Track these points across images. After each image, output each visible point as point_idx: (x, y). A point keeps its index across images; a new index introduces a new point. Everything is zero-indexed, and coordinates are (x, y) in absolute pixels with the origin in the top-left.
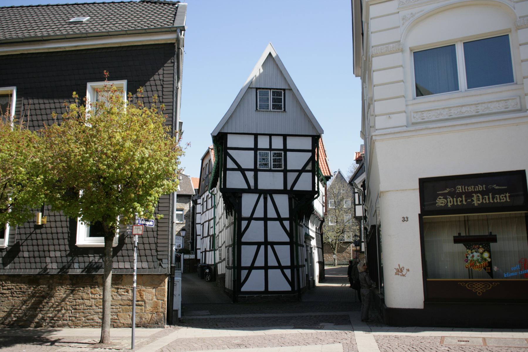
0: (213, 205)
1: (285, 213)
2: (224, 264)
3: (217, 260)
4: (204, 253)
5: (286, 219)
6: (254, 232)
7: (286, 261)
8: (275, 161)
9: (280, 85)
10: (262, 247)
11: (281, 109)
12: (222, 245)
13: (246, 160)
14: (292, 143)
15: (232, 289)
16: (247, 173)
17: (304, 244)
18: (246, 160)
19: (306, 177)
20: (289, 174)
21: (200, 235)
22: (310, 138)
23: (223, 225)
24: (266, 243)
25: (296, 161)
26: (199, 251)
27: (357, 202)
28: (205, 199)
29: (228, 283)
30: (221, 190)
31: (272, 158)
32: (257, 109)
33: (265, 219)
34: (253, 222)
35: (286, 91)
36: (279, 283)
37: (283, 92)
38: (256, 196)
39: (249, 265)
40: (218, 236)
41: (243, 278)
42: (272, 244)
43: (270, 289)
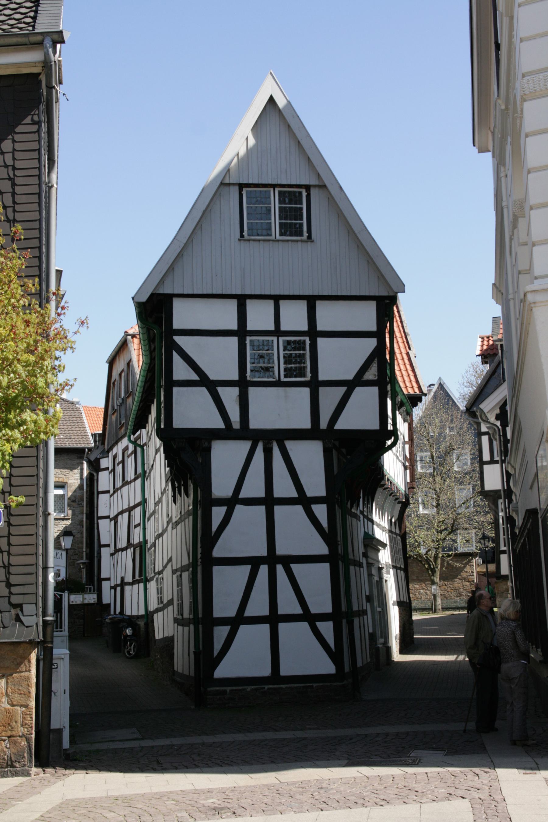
0: (139, 470)
1: (315, 486)
2: (170, 613)
3: (153, 605)
5: (318, 500)
7: (321, 601)
8: (288, 359)
9: (298, 176)
10: (264, 570)
11: (301, 235)
12: (165, 567)
13: (220, 359)
14: (329, 316)
15: (192, 674)
16: (221, 390)
17: (363, 560)
18: (220, 359)
19: (365, 398)
20: (323, 391)
21: (108, 546)
22: (372, 305)
23: (165, 520)
24: (272, 559)
25: (338, 359)
26: (106, 585)
27: (486, 457)
28: (120, 458)
29: (182, 660)
30: (160, 433)
32: (242, 236)
33: (269, 501)
34: (239, 508)
35: (313, 191)
36: (305, 655)
37: (304, 194)
38: (245, 446)
39: (232, 613)
40: (154, 545)
41: (217, 647)
42: (288, 561)
43: (284, 671)
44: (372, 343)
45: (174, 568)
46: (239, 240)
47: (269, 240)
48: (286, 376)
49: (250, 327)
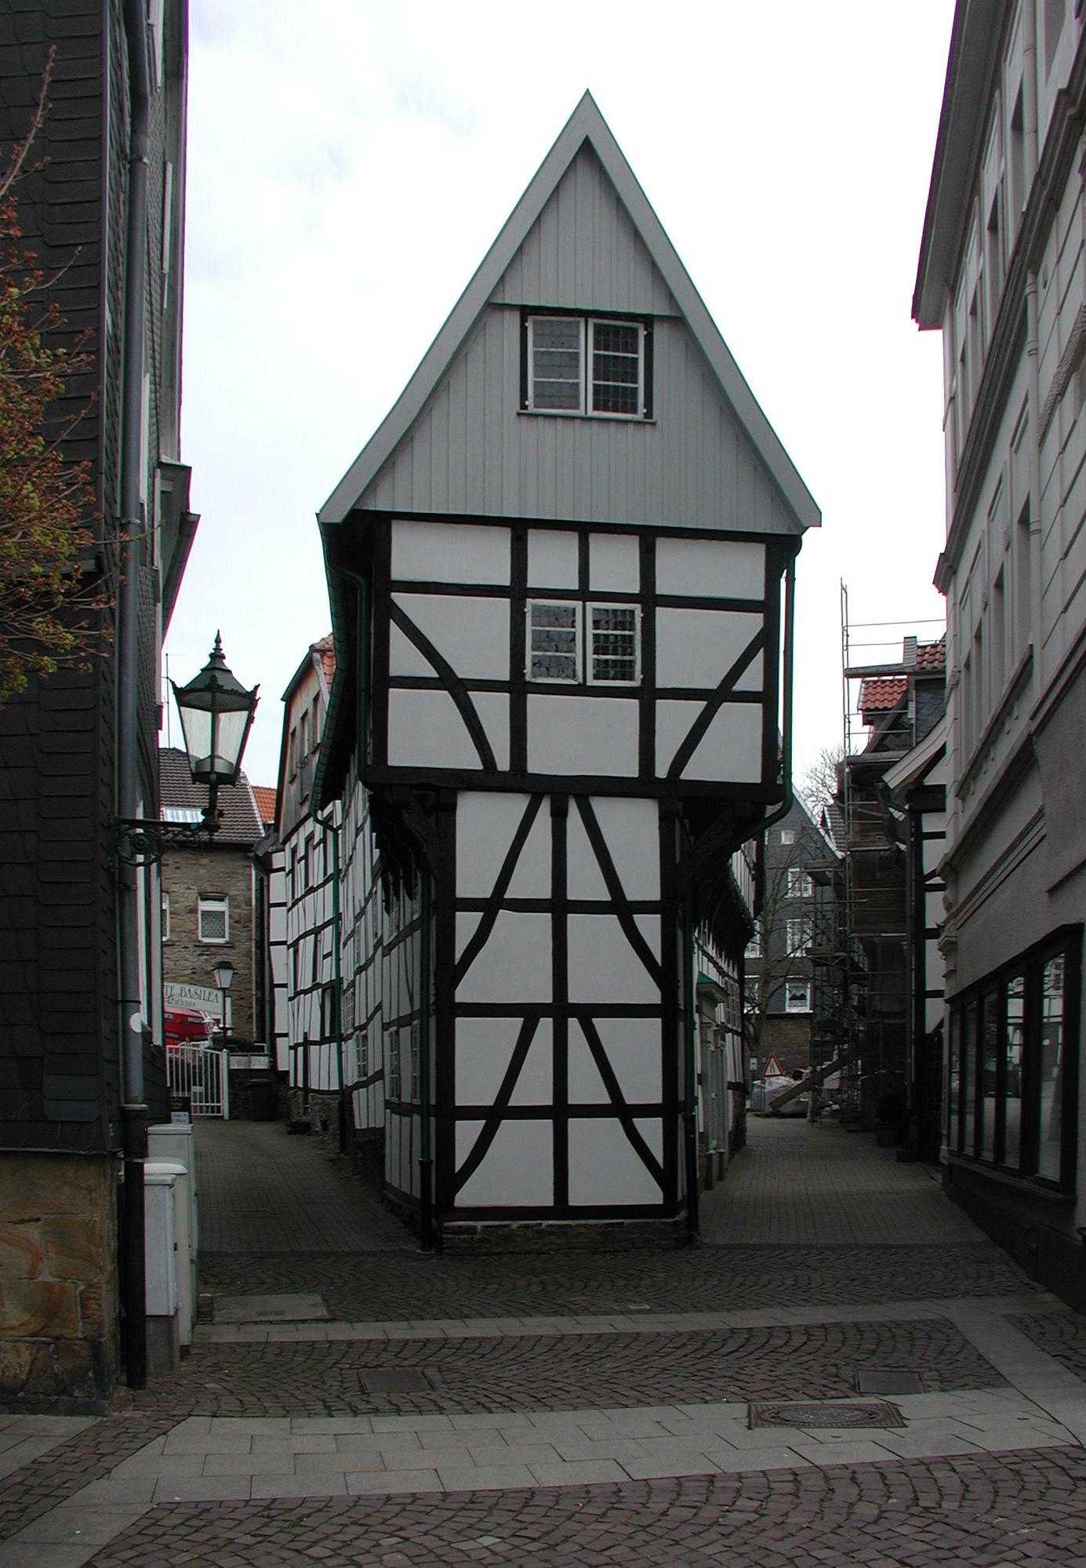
1: (643, 879)
2: (379, 1092)
4: (301, 1049)
6: (509, 963)
9: (631, 296)
10: (546, 1025)
11: (634, 411)
12: (370, 1019)
13: (476, 639)
18: (476, 639)
24: (560, 1009)
25: (692, 648)
29: (401, 1169)
31: (590, 631)
32: (524, 407)
35: (661, 333)
36: (611, 1172)
37: (642, 333)
38: (518, 804)
40: (353, 984)
42: (587, 1013)
44: (755, 622)
45: (386, 1020)
46: (519, 414)
47: (573, 418)
48: (596, 677)
49: (532, 582)
